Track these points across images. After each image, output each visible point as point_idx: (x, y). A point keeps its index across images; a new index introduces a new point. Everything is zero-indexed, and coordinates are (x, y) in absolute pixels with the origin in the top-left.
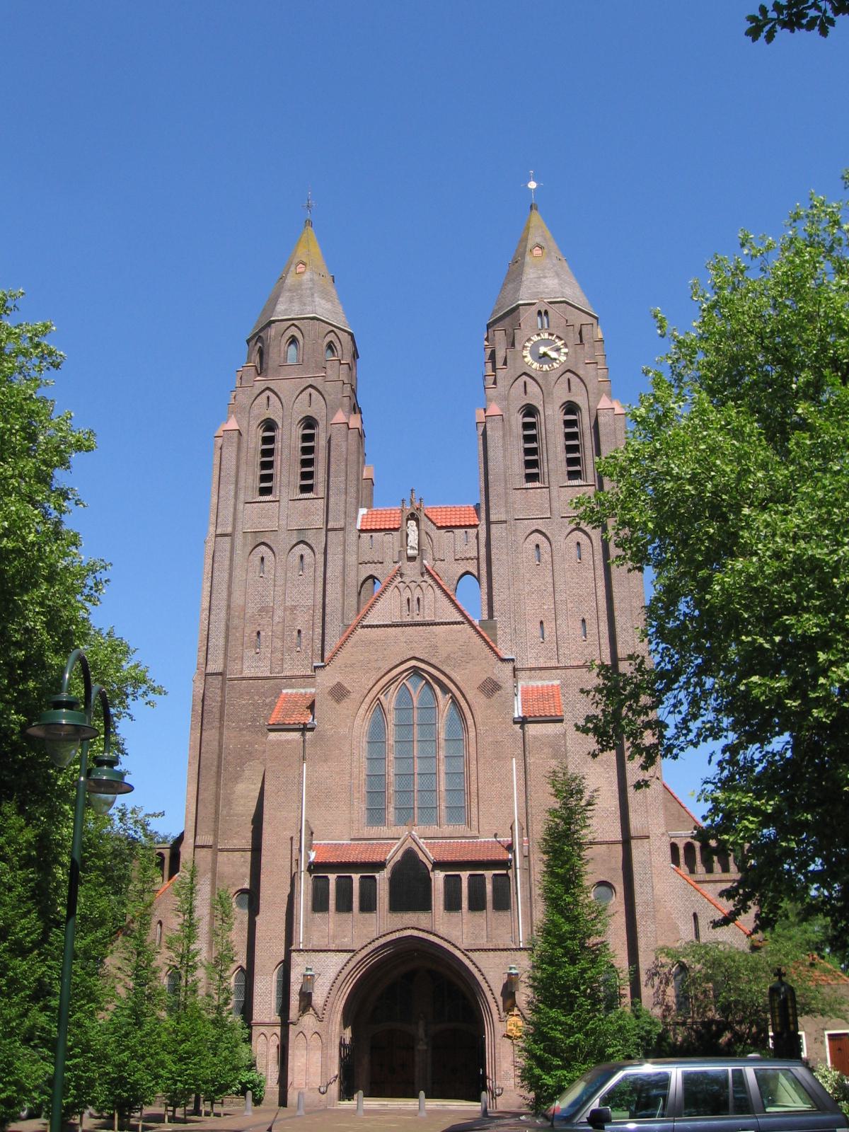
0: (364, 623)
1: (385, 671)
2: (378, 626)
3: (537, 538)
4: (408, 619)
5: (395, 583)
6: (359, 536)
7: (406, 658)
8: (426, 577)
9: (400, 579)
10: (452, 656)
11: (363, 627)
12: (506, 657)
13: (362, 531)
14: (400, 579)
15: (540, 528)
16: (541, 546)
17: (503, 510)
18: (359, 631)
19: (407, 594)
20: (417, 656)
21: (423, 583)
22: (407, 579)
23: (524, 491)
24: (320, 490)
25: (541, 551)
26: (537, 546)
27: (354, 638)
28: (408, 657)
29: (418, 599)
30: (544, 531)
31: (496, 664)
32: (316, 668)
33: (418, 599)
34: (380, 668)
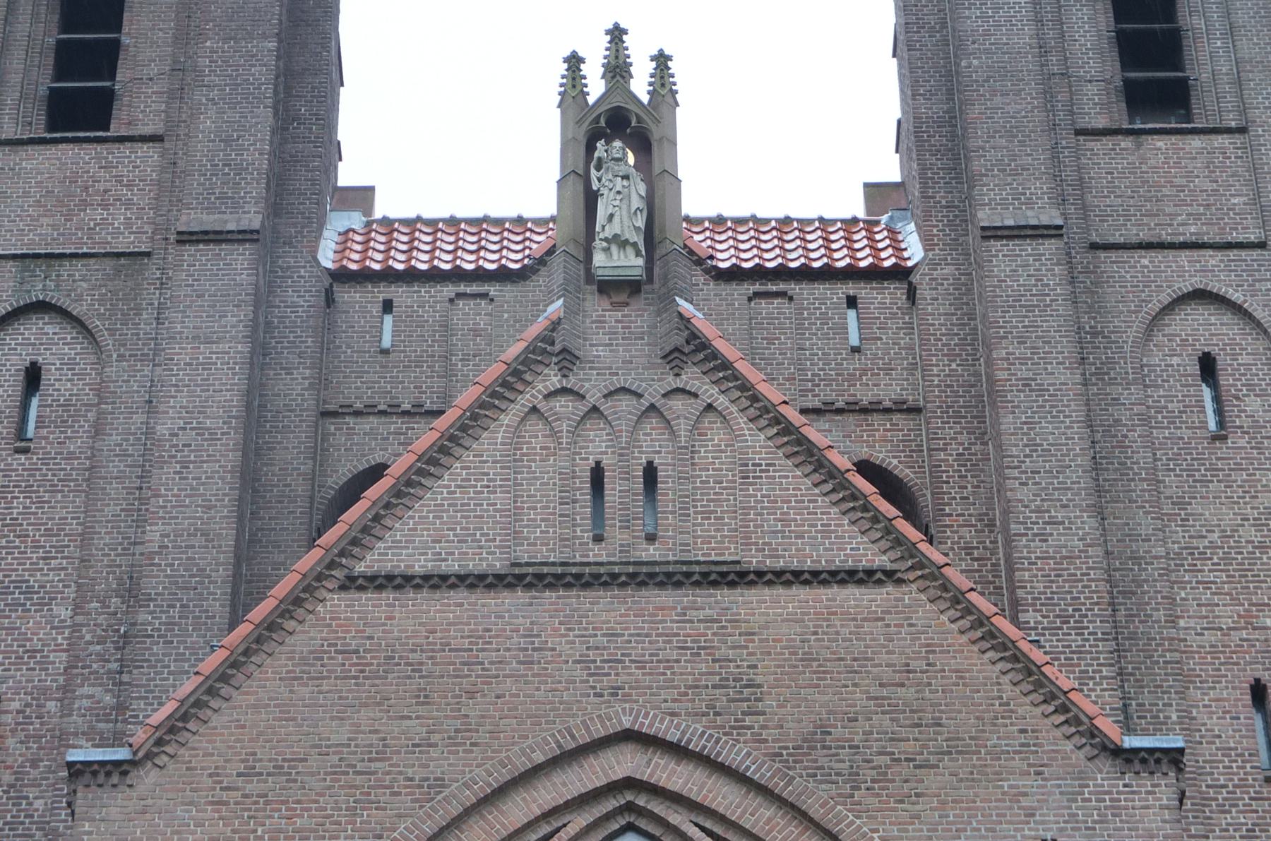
0: (360, 568)
1: (470, 797)
2: (437, 582)
3: (1202, 328)
4: (598, 554)
5: (531, 396)
6: (330, 300)
7: (583, 738)
8: (691, 377)
9: (554, 380)
10: (837, 732)
11: (351, 583)
12: (1130, 742)
13: (341, 276)
14: (554, 380)
15: (1214, 287)
16: (1222, 361)
17: (1039, 188)
18: (334, 603)
19: (597, 445)
20: (646, 725)
21: (678, 404)
22: (593, 386)
23: (1126, 143)
24: (140, 100)
25: (1224, 381)
26: (1208, 367)
27: (305, 636)
28: (599, 731)
29: (650, 474)
30: (1237, 297)
31: (1082, 776)
32: (77, 771)
33: (650, 474)
34: (440, 783)
